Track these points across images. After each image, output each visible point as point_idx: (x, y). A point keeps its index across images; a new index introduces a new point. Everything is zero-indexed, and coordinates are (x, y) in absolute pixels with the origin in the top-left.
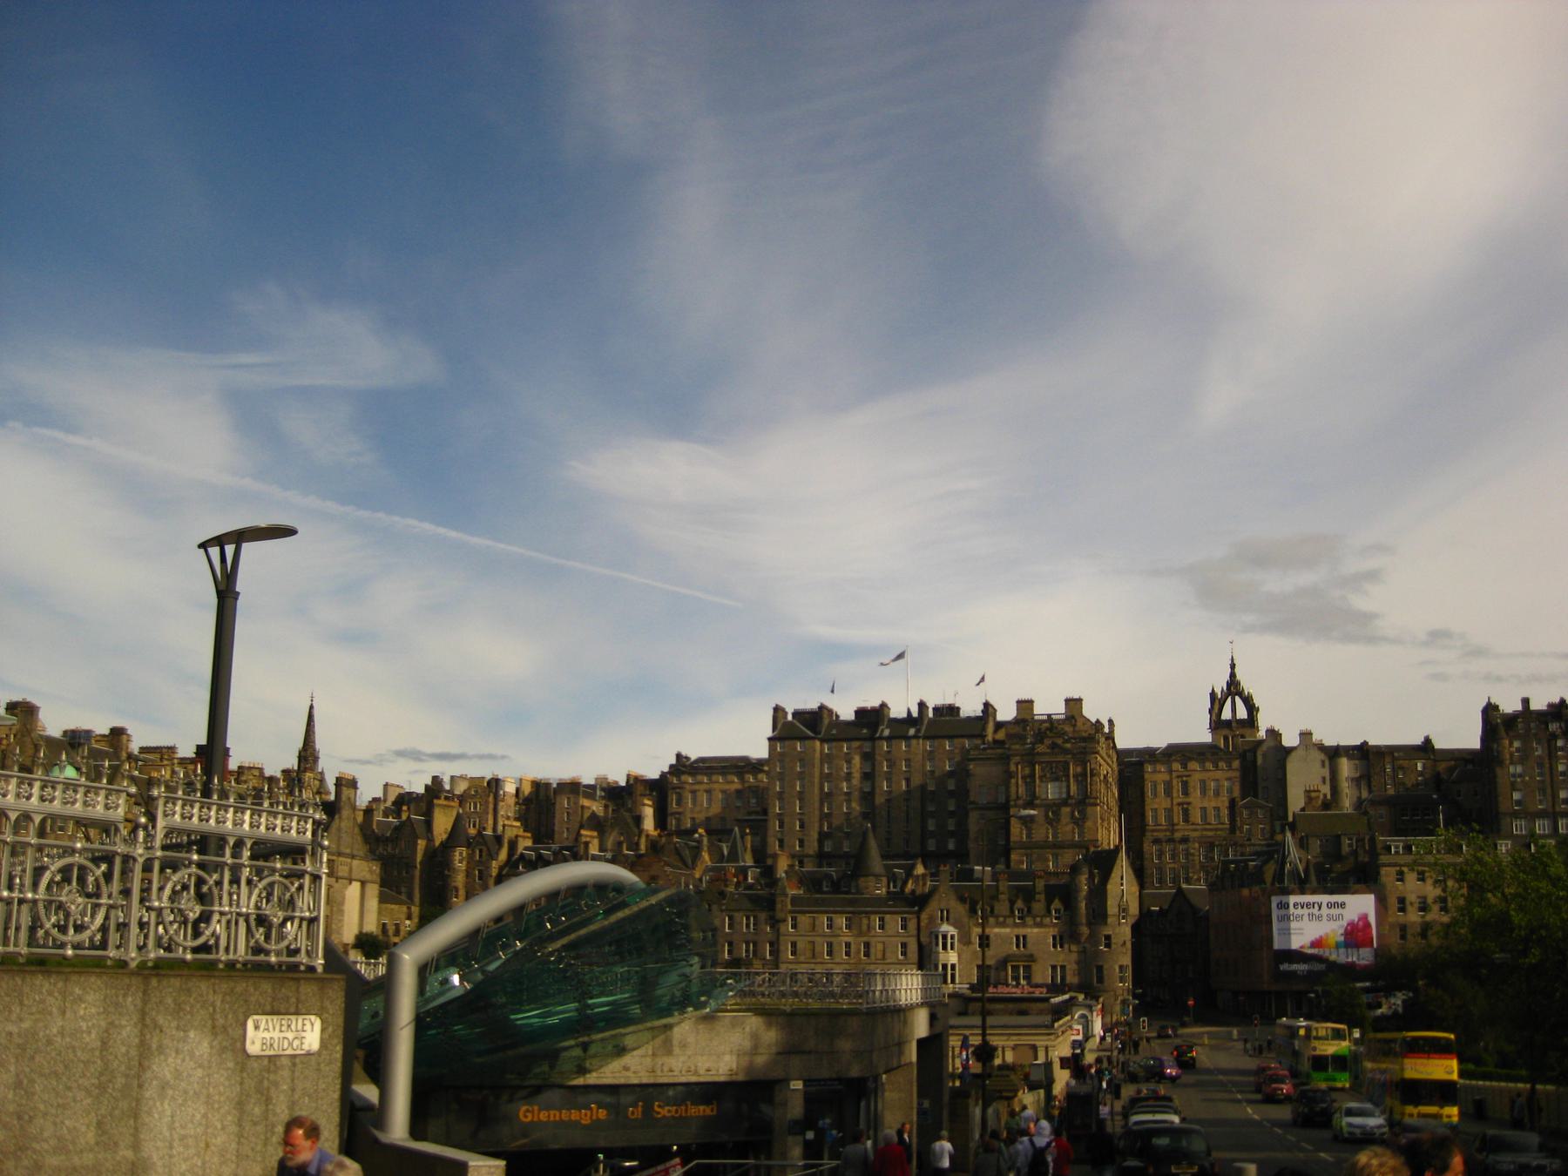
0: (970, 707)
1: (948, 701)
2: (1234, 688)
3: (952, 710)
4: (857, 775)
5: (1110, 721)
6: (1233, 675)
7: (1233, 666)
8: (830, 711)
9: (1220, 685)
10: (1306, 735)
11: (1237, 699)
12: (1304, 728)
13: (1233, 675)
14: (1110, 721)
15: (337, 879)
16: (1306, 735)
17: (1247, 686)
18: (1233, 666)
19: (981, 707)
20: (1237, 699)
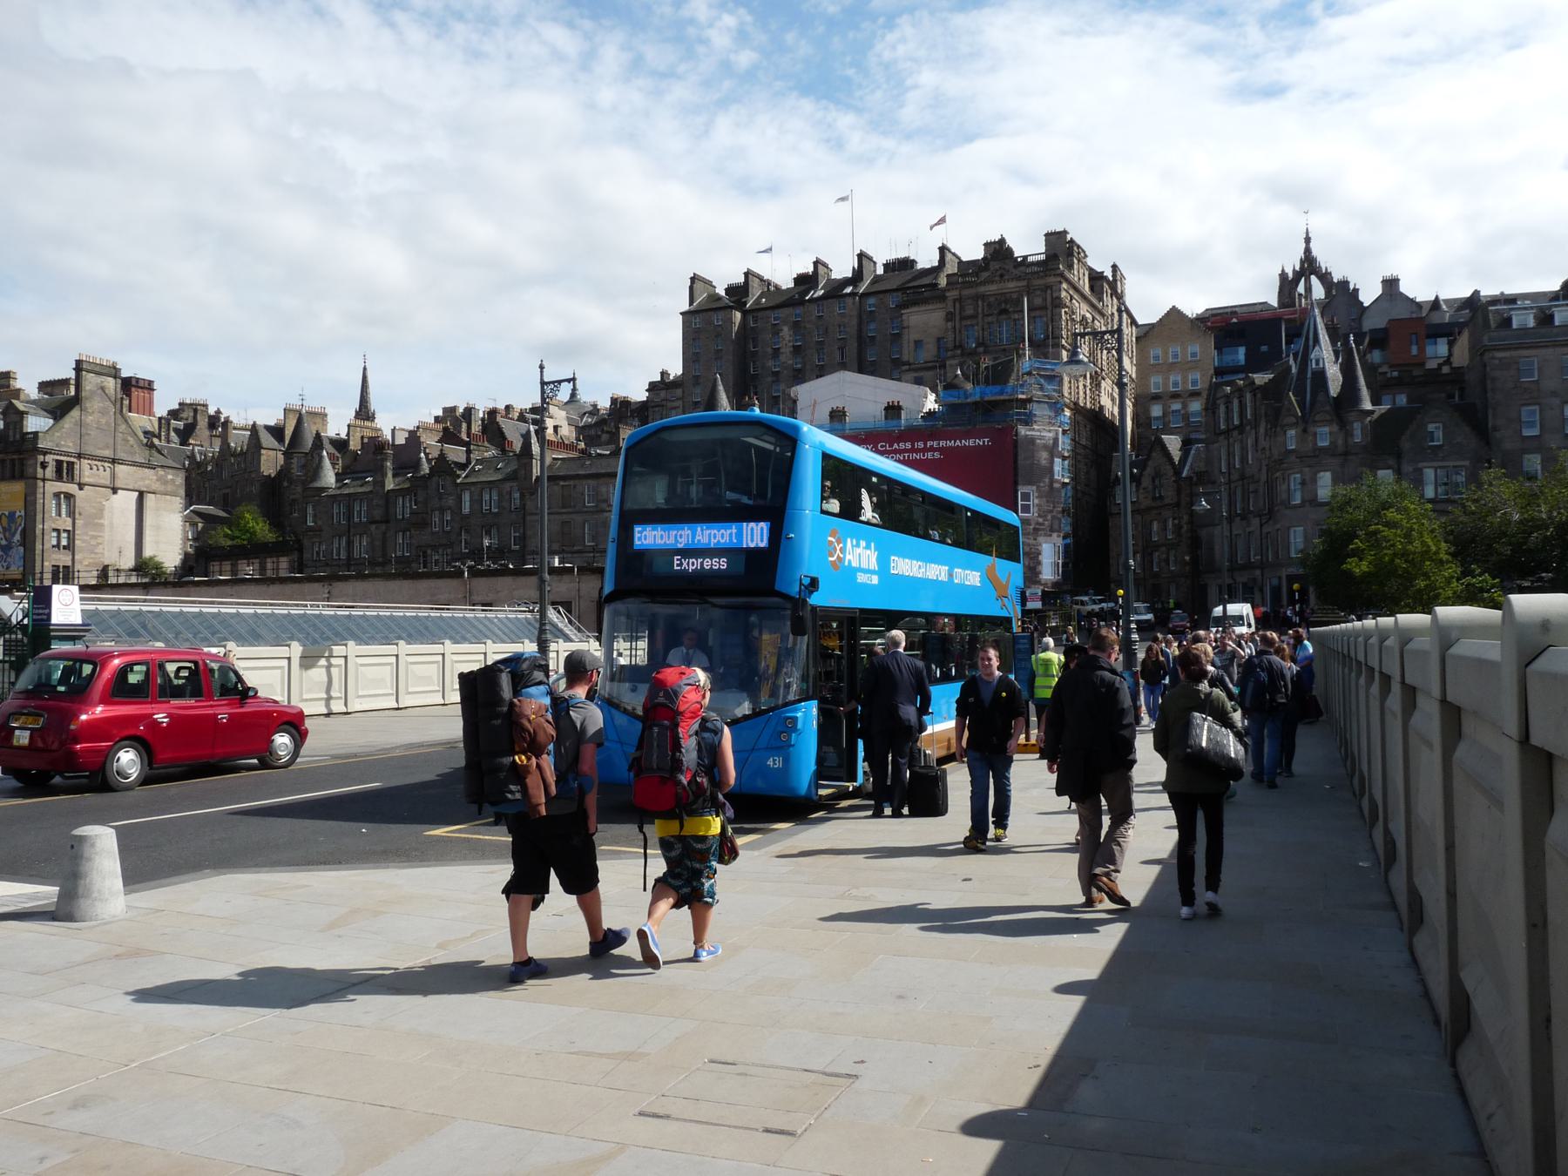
0: (926, 259)
1: (901, 255)
2: (1309, 265)
3: (905, 264)
4: (786, 351)
5: (1115, 267)
6: (1308, 251)
7: (1308, 240)
8: (761, 279)
9: (1292, 263)
10: (1391, 284)
11: (1313, 278)
12: (1388, 274)
13: (1308, 251)
14: (1115, 267)
15: (81, 486)
16: (1391, 284)
17: (1324, 259)
18: (1308, 240)
19: (937, 257)
20: (1313, 278)
